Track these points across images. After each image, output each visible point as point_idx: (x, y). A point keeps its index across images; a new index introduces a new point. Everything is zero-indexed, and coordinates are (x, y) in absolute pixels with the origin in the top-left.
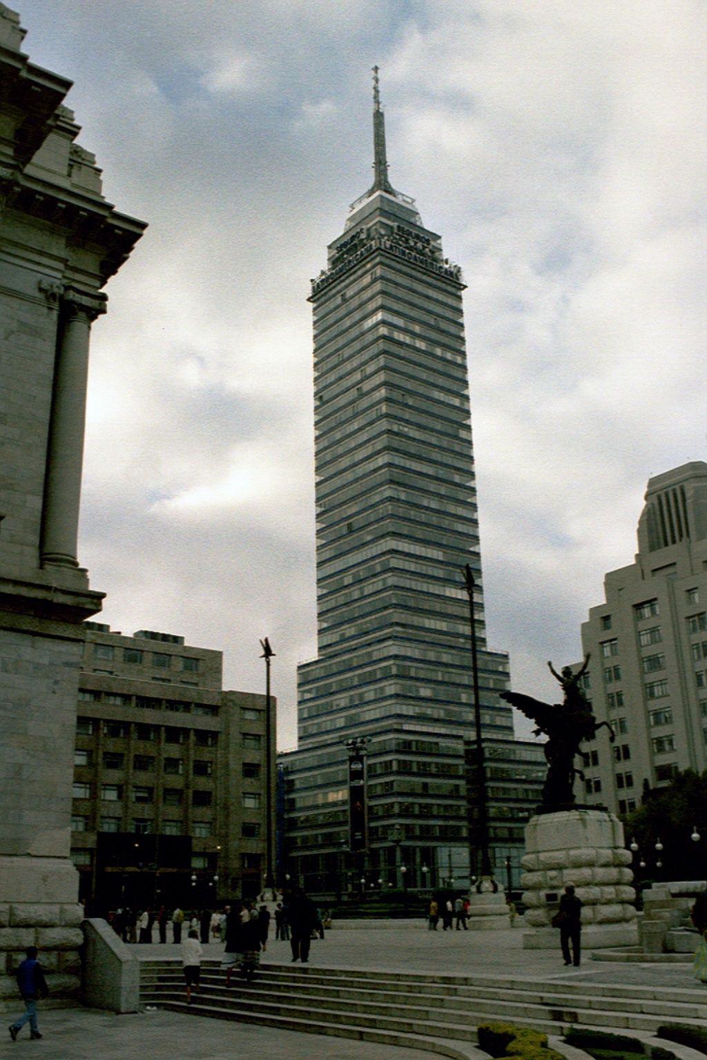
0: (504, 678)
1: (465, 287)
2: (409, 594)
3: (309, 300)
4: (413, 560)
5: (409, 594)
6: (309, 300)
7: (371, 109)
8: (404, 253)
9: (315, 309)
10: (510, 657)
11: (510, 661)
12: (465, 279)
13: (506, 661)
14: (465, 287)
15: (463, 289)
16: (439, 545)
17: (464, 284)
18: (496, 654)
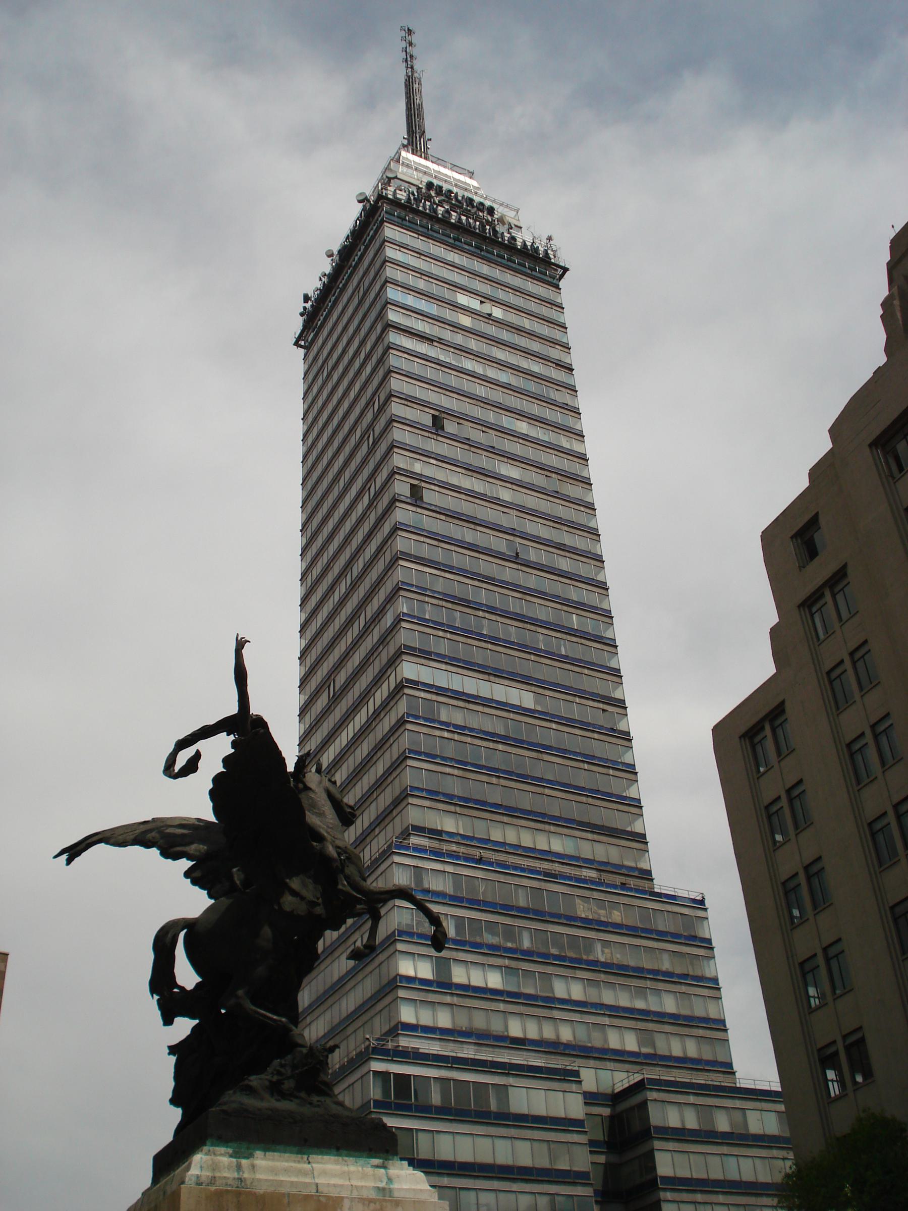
0: (701, 952)
1: (565, 270)
2: (448, 770)
3: (297, 344)
4: (461, 704)
5: (448, 770)
6: (297, 344)
7: (401, 74)
8: (435, 211)
9: (305, 355)
10: (708, 903)
11: (710, 914)
12: (563, 258)
13: (700, 913)
14: (565, 270)
15: (562, 276)
16: (525, 681)
17: (562, 264)
18: (674, 897)
